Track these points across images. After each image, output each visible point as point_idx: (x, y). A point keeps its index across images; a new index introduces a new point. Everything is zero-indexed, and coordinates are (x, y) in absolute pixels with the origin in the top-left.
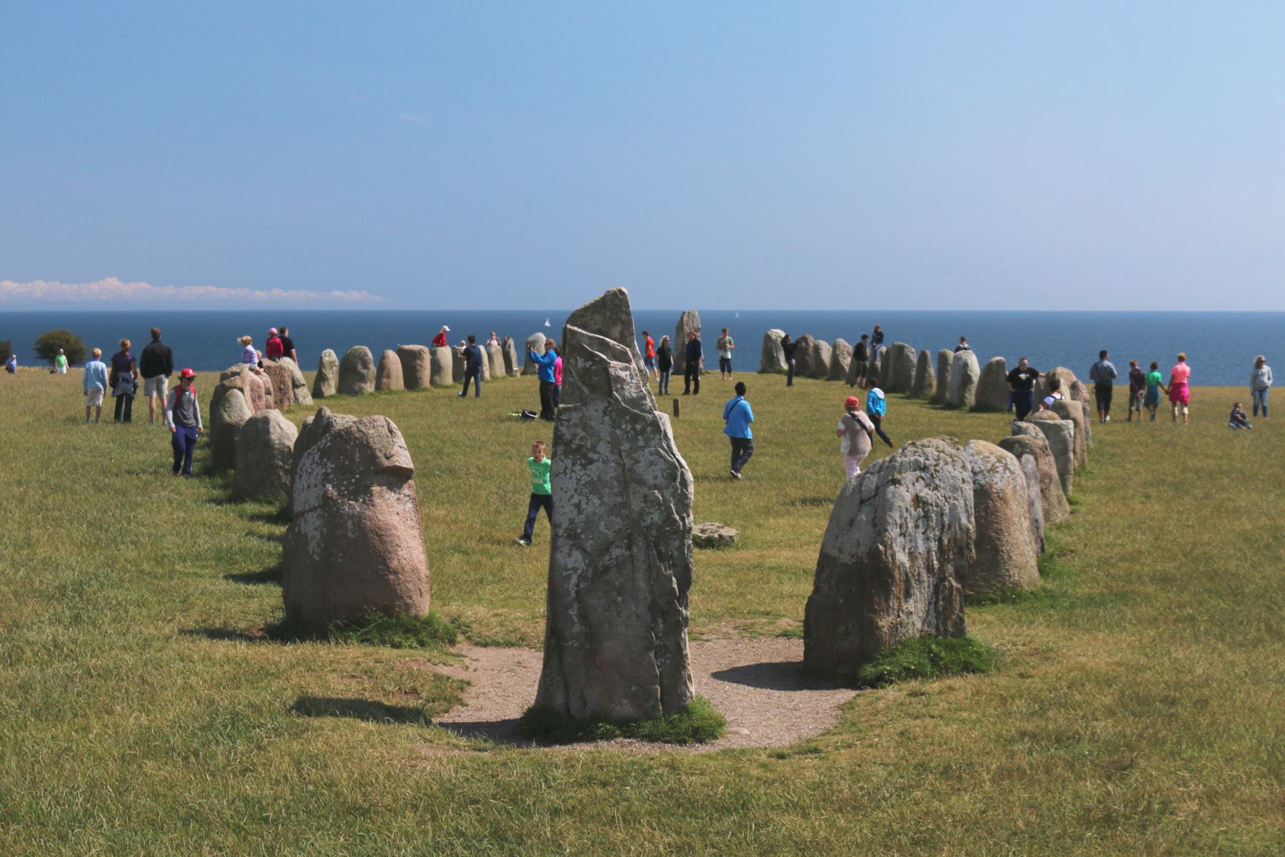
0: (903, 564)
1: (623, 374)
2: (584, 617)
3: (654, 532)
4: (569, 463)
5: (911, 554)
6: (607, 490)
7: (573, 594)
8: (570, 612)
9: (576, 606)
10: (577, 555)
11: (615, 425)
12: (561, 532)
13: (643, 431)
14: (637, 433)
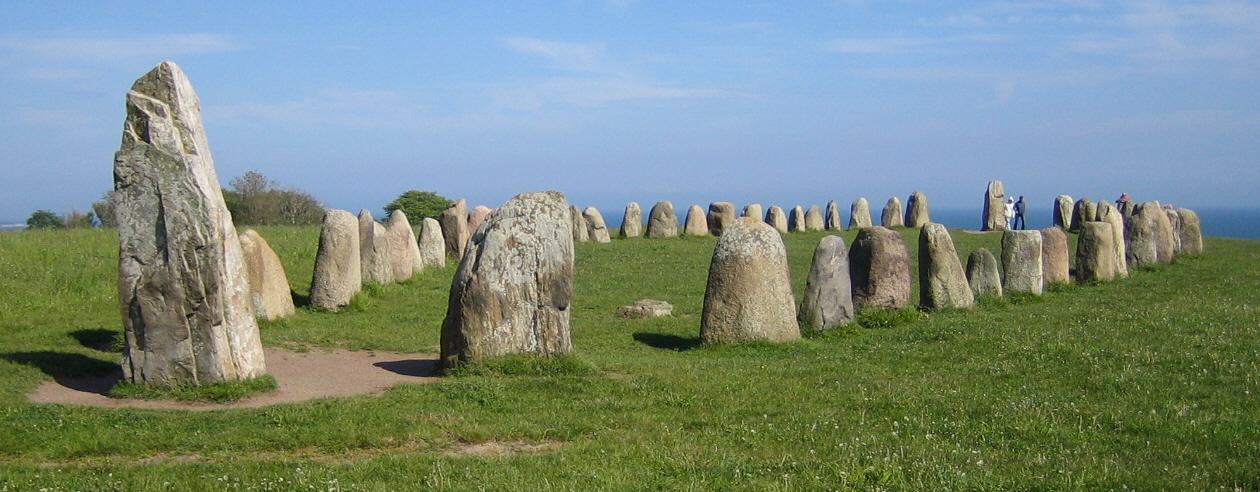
0: (498, 293)
1: (158, 126)
4: (126, 193)
5: (507, 285)
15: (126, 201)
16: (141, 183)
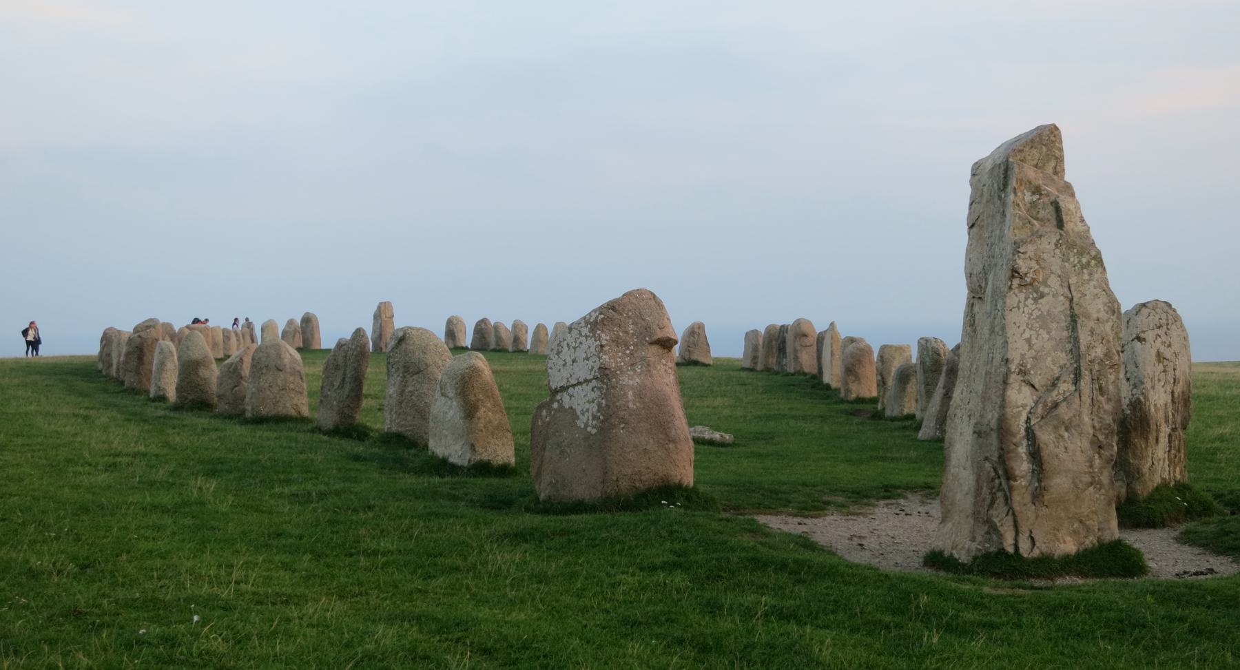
2: (1036, 455)
3: (1097, 367)
4: (1022, 296)
6: (1055, 325)
7: (1023, 432)
8: (1020, 450)
9: (1025, 442)
10: (1026, 390)
11: (1065, 259)
12: (1013, 367)
13: (1088, 263)
14: (1083, 267)
15: (1021, 305)
16: (1045, 283)
